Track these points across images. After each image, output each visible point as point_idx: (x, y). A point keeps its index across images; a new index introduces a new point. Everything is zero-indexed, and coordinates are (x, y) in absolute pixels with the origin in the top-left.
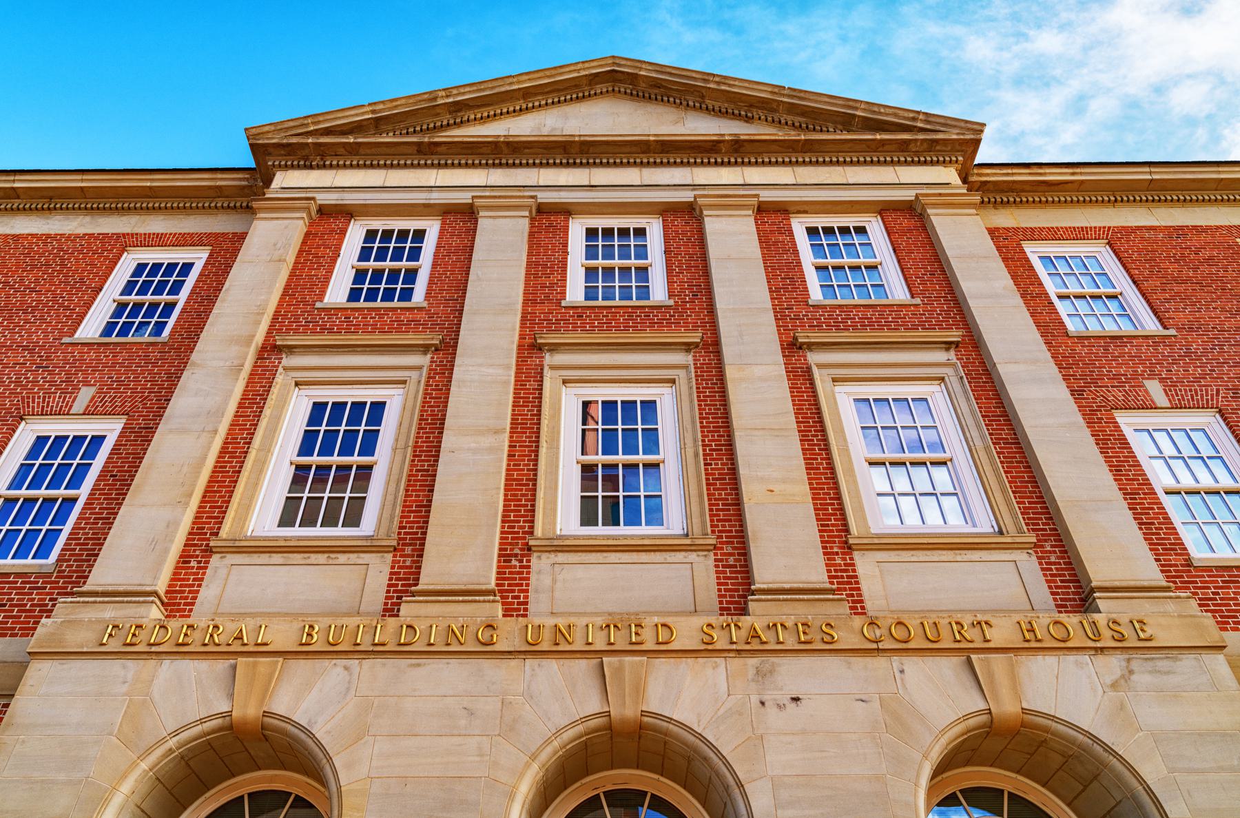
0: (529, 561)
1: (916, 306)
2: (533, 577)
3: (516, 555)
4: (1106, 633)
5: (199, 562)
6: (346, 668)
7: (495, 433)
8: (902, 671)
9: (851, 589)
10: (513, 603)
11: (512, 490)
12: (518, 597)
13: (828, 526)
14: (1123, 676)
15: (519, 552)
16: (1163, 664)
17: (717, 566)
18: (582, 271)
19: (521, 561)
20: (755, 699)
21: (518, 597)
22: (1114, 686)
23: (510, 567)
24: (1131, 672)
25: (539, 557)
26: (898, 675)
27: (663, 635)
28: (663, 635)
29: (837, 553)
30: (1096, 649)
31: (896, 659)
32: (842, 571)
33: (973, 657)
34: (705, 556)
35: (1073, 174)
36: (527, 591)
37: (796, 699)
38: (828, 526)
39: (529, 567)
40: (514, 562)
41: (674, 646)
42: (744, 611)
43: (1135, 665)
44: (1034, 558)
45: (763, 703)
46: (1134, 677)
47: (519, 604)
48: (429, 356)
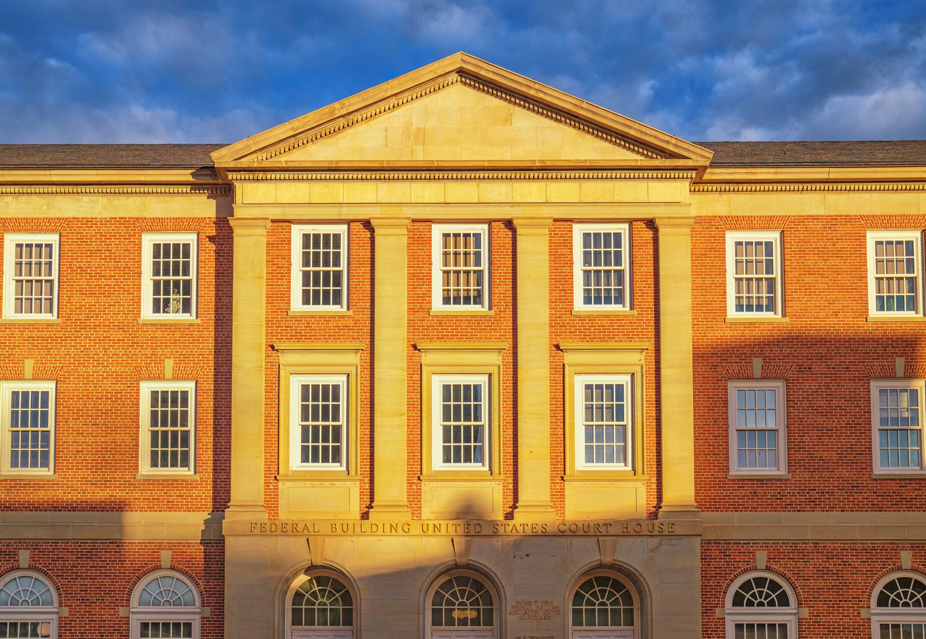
0: (420, 486)
1: (633, 316)
2: (423, 494)
3: (415, 483)
4: (657, 529)
5: (274, 486)
6: (352, 541)
7: (401, 415)
8: (571, 544)
9: (561, 501)
10: (415, 507)
11: (410, 446)
12: (417, 504)
13: (556, 468)
14: (657, 547)
15: (415, 487)
16: (674, 542)
17: (504, 489)
18: (441, 428)
19: (417, 486)
20: (512, 555)
21: (417, 504)
22: (652, 550)
23: (412, 489)
24: (661, 545)
25: (425, 484)
26: (569, 545)
27: (478, 529)
28: (478, 529)
29: (558, 483)
30: (650, 535)
31: (570, 539)
32: (558, 492)
33: (600, 538)
34: (499, 484)
35: (776, 173)
36: (420, 501)
37: (528, 555)
38: (556, 468)
39: (420, 489)
40: (414, 487)
41: (482, 533)
42: (512, 518)
43: (663, 542)
44: (645, 486)
45: (515, 557)
46: (661, 547)
47: (417, 507)
48: (359, 355)
